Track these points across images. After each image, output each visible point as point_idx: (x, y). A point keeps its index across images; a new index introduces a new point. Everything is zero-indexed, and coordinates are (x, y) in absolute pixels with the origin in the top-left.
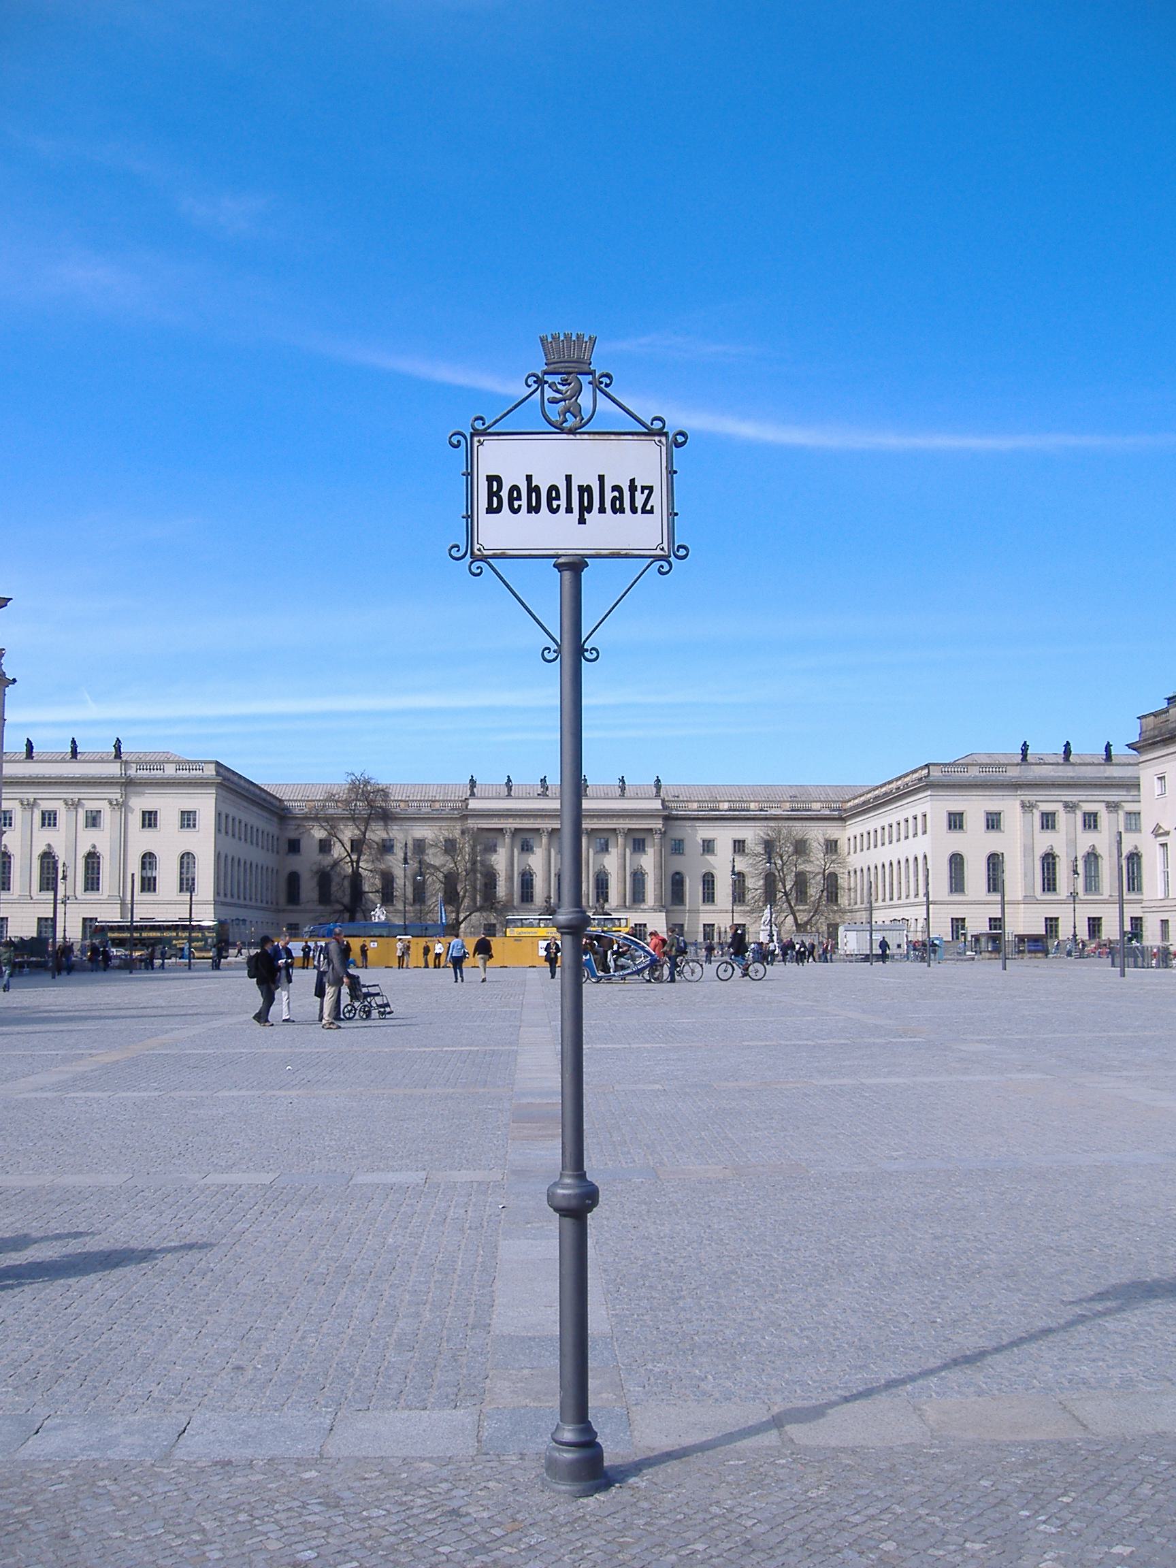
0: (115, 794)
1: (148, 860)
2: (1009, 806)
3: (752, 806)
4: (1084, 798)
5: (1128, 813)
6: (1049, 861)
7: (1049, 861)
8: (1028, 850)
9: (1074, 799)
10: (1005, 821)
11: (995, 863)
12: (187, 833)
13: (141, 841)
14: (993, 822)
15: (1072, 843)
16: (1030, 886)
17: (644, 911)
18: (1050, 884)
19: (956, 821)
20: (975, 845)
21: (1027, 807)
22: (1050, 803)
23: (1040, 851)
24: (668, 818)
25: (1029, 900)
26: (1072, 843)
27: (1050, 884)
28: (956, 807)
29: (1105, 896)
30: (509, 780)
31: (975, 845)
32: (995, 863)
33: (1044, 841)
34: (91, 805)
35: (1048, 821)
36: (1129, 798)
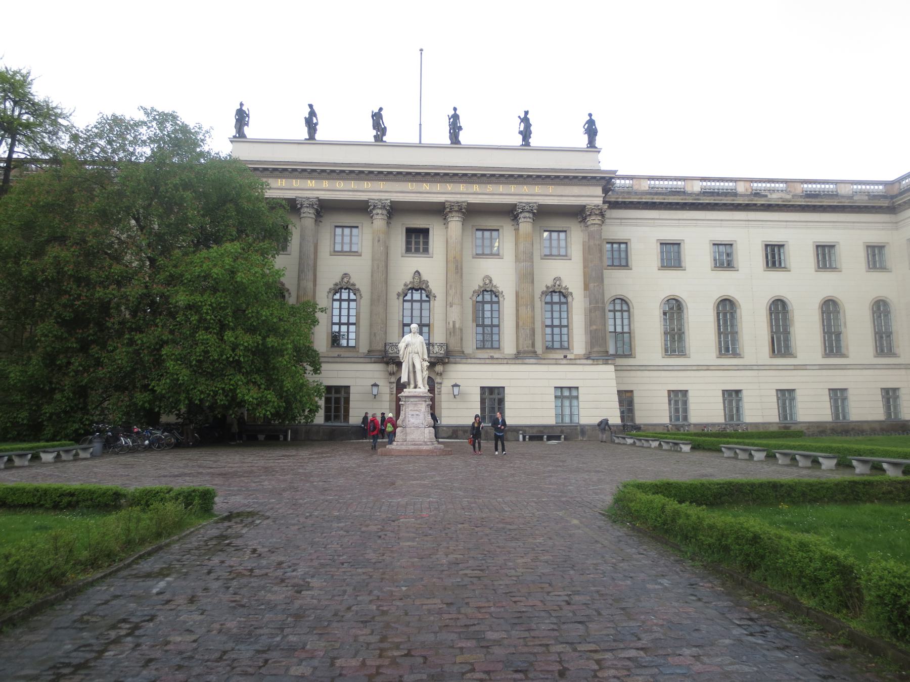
17: (573, 362)
30: (312, 113)
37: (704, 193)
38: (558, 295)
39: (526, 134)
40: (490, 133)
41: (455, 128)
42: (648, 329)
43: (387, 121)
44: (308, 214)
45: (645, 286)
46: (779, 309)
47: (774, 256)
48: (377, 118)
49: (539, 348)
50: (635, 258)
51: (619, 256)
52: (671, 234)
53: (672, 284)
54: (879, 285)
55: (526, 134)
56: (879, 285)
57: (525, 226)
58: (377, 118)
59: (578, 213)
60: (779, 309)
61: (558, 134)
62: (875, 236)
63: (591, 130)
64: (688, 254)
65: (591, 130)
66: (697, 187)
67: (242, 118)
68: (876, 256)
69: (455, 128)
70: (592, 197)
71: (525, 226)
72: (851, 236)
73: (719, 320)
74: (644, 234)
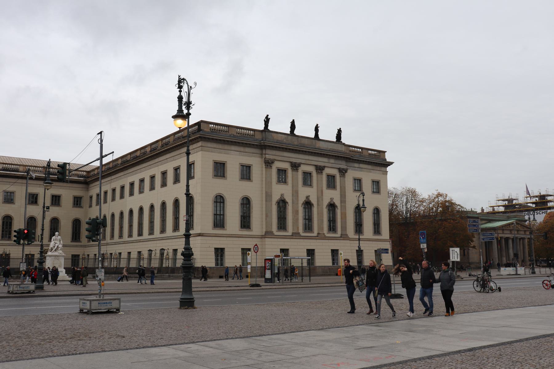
3: (21, 169)
4: (303, 161)
8: (268, 196)
9: (298, 161)
11: (246, 203)
14: (246, 173)
15: (295, 193)
16: (269, 224)
18: (282, 224)
19: (220, 169)
20: (233, 189)
21: (268, 163)
23: (276, 198)
26: (295, 193)
27: (282, 224)
28: (220, 157)
31: (233, 189)
32: (246, 203)
36: (330, 165)
37: (4, 169)
54: (77, 213)
56: (77, 213)
68: (77, 202)
72: (67, 193)
73: (3, 225)
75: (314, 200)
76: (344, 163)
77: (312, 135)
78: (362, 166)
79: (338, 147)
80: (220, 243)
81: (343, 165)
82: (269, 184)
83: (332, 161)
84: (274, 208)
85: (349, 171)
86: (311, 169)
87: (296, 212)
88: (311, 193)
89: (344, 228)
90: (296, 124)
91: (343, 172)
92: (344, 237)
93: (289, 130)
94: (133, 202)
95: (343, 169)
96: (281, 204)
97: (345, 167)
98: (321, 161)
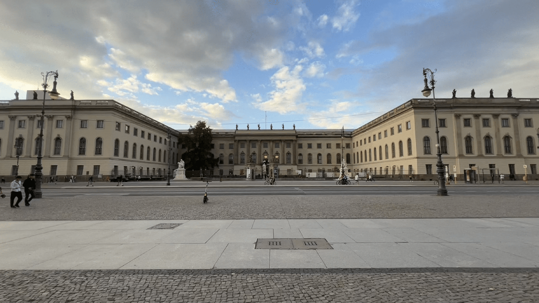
0: (69, 113)
1: (83, 141)
2: (450, 117)
3: (323, 133)
5: (503, 119)
6: (469, 139)
7: (469, 139)
8: (459, 135)
10: (447, 123)
12: (99, 130)
13: (80, 133)
14: (442, 123)
15: (478, 132)
16: (460, 150)
18: (469, 149)
21: (458, 116)
22: (468, 114)
23: (464, 135)
24: (297, 137)
25: (461, 156)
26: (478, 132)
27: (469, 149)
29: (495, 155)
33: (466, 131)
34: (59, 118)
35: (467, 123)
38: (289, 154)
39: (283, 127)
40: (277, 127)
41: (271, 127)
42: (305, 158)
43: (260, 126)
44: (248, 142)
45: (305, 151)
46: (329, 155)
47: (329, 146)
48: (259, 125)
49: (285, 163)
50: (303, 147)
51: (300, 146)
52: (310, 142)
53: (310, 151)
55: (283, 127)
56: (347, 151)
57: (283, 143)
58: (259, 125)
59: (292, 140)
60: (329, 155)
61: (289, 127)
62: (348, 142)
63: (294, 127)
64: (312, 145)
65: (294, 127)
66: (315, 133)
67: (237, 126)
69: (271, 127)
70: (294, 138)
71: (283, 143)
74: (305, 143)
75: (493, 135)
76: (515, 110)
77: (489, 96)
78: (531, 110)
79: (510, 101)
80: (429, 162)
81: (515, 111)
82: (458, 128)
83: (506, 110)
84: (464, 142)
85: (520, 115)
86: (490, 117)
87: (479, 143)
88: (491, 131)
89: (519, 150)
90: (475, 91)
91: (515, 116)
92: (519, 156)
93: (471, 95)
94: (376, 144)
95: (516, 114)
96: (468, 139)
97: (516, 112)
98: (496, 111)
